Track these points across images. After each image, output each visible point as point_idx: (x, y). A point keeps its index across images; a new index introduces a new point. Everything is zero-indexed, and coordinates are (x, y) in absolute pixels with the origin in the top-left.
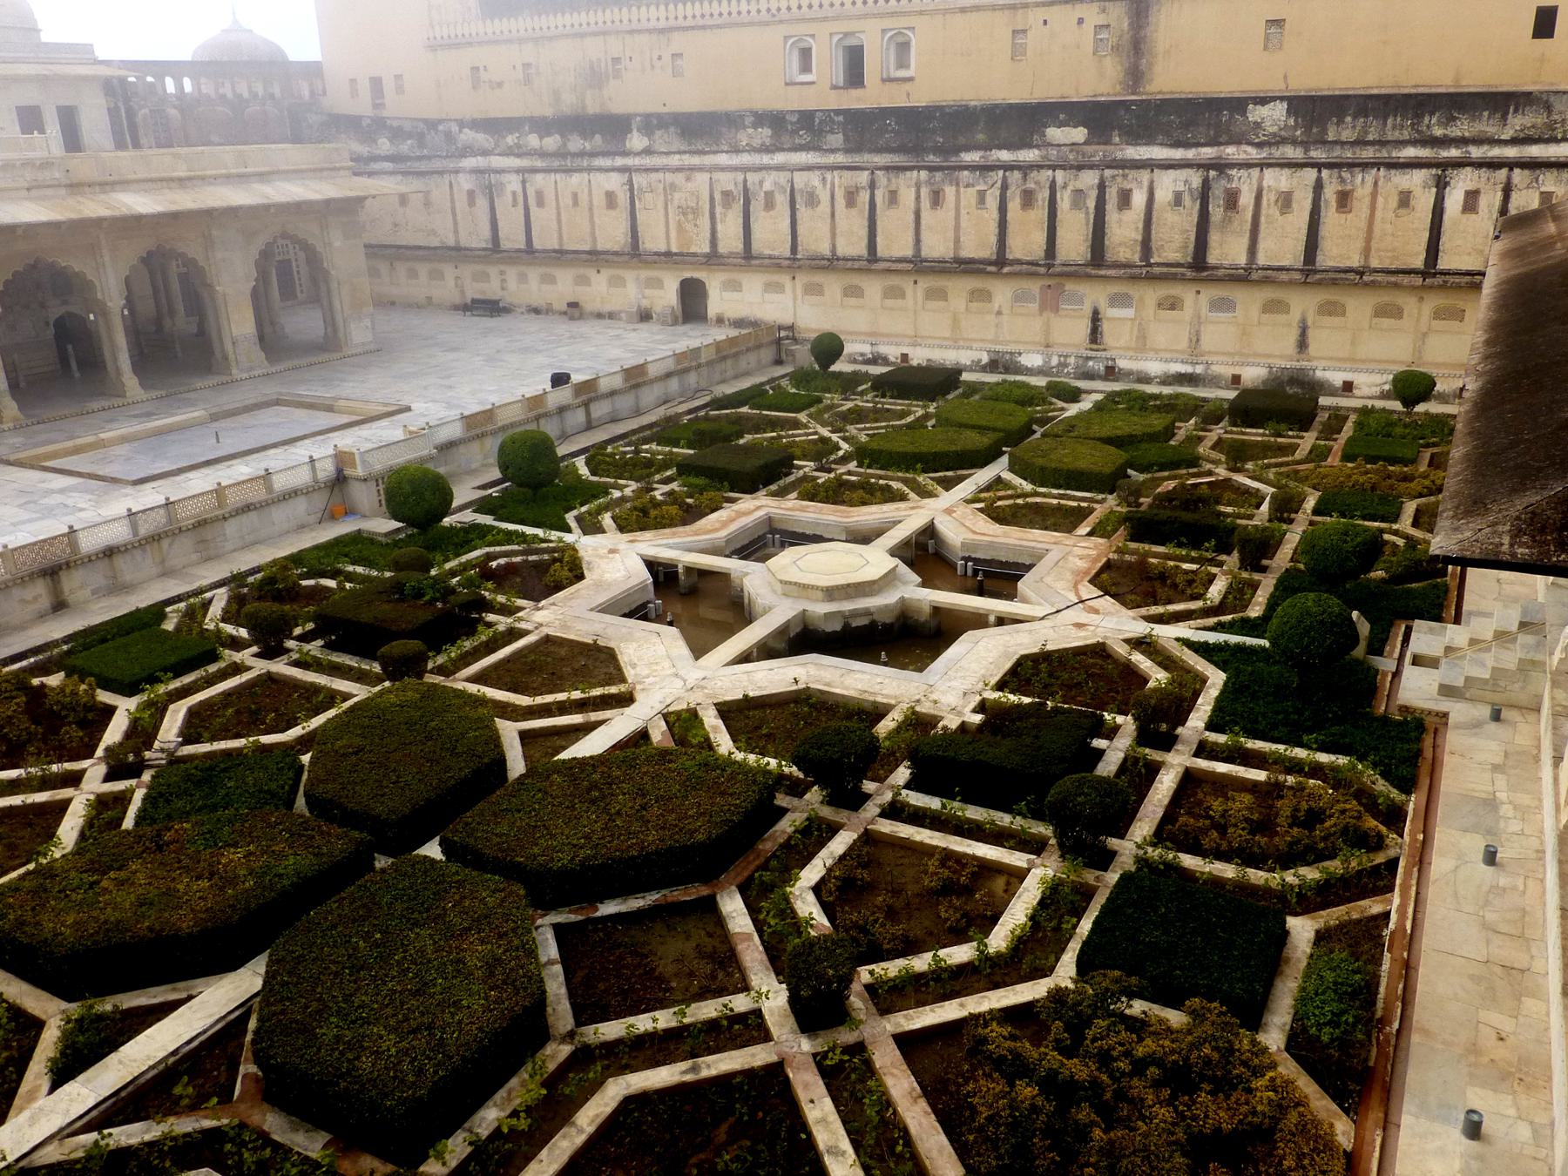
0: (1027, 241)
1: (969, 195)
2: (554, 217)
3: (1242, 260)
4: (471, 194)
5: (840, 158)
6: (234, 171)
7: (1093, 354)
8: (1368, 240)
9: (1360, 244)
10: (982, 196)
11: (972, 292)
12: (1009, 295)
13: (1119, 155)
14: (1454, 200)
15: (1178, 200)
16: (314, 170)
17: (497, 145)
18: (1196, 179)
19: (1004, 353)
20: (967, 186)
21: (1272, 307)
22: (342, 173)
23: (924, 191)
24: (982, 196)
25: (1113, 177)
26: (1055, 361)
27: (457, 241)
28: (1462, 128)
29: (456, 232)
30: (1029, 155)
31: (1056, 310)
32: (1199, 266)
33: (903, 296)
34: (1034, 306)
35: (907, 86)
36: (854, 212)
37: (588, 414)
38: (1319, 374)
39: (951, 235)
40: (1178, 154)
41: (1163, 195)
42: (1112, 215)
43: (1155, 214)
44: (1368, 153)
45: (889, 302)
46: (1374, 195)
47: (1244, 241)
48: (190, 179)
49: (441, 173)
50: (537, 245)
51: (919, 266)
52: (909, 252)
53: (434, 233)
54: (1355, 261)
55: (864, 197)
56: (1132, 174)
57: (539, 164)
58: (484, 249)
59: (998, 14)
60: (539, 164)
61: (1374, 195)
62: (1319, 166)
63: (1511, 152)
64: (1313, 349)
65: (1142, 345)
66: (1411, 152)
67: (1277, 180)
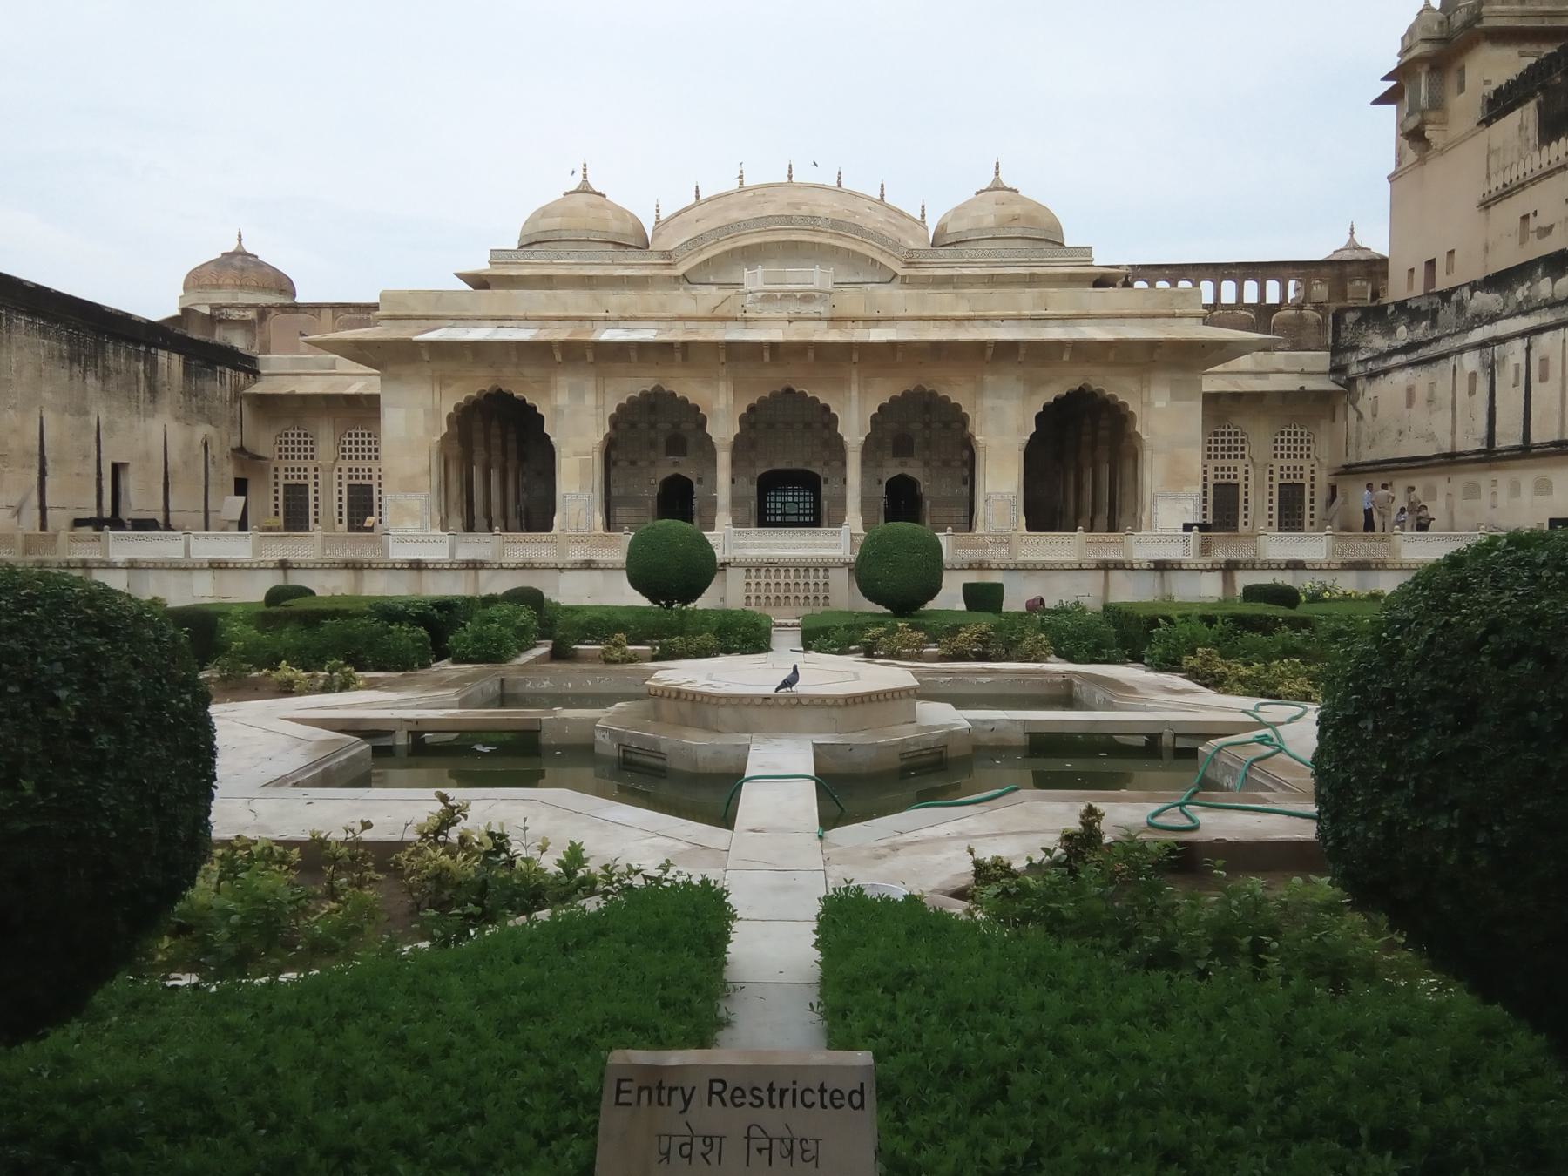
2: (1558, 394)
4: (1473, 375)
6: (1027, 312)
16: (1142, 316)
17: (1505, 305)
22: (1186, 320)
27: (1453, 446)
29: (1453, 432)
37: (1228, 583)
48: (969, 319)
49: (1445, 356)
50: (1536, 438)
53: (1431, 437)
57: (1547, 318)
58: (1478, 452)
60: (1547, 318)
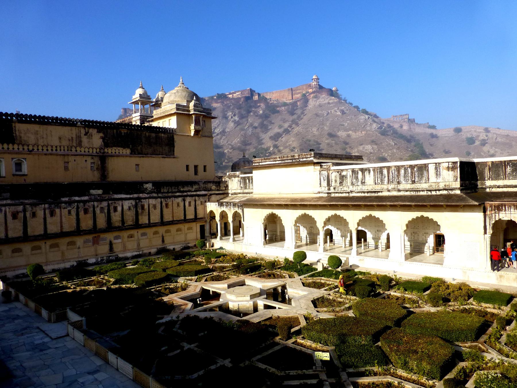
0: (87, 223)
1: (65, 212)
3: (147, 222)
5: (9, 202)
7: (112, 255)
8: (173, 214)
9: (171, 215)
10: (69, 212)
11: (68, 243)
12: (82, 241)
13: (113, 197)
14: (187, 204)
15: (130, 208)
18: (133, 202)
19: (82, 261)
20: (64, 208)
21: (156, 233)
23: (47, 212)
24: (69, 212)
25: (112, 203)
26: (99, 260)
28: (186, 189)
30: (86, 198)
31: (98, 243)
32: (137, 226)
33: (40, 248)
34: (91, 244)
35: (25, 177)
36: (16, 221)
38: (168, 247)
39: (59, 225)
40: (128, 196)
41: (126, 207)
42: (112, 214)
43: (124, 213)
44: (170, 194)
45: (34, 252)
46: (172, 204)
47: (147, 217)
51: (46, 236)
52: (42, 233)
54: (171, 219)
55: (21, 215)
56: (117, 202)
59: (59, 157)
61: (172, 204)
62: (161, 198)
63: (195, 193)
64: (166, 242)
65: (125, 250)
66: (178, 194)
67: (152, 202)
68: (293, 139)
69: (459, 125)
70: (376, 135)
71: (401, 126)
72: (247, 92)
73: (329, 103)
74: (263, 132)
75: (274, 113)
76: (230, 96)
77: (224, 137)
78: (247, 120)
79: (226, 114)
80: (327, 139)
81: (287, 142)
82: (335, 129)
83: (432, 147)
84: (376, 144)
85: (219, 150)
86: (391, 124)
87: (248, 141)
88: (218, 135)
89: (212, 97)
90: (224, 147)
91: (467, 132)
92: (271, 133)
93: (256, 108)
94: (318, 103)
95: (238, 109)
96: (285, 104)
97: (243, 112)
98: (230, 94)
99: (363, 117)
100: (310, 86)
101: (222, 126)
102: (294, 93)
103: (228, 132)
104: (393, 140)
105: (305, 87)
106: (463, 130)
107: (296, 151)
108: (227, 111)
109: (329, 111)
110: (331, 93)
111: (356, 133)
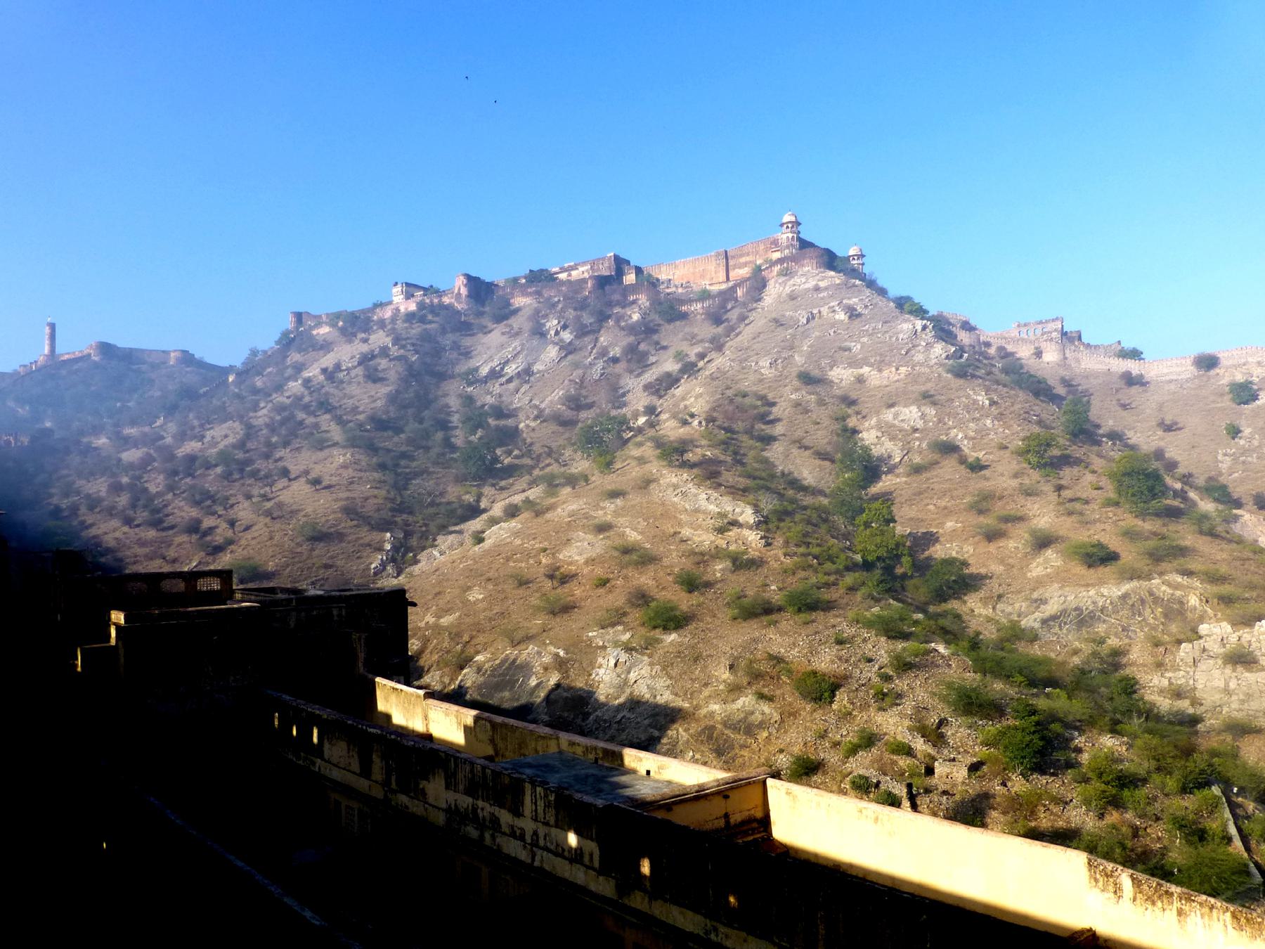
68: (699, 390)
69: (1209, 349)
70: (940, 375)
71: (1039, 354)
72: (606, 265)
73: (817, 289)
74: (631, 372)
75: (670, 321)
76: (563, 276)
77: (525, 387)
78: (597, 340)
79: (544, 325)
80: (797, 390)
81: (683, 399)
82: (824, 362)
83: (1125, 413)
84: (934, 404)
85: (502, 423)
86: (1010, 348)
87: (586, 397)
88: (510, 380)
89: (515, 280)
90: (521, 416)
91: (1236, 367)
92: (650, 376)
93: (623, 307)
94: (788, 290)
95: (575, 309)
96: (705, 295)
97: (588, 319)
98: (563, 270)
99: (907, 326)
100: (775, 243)
101: (527, 355)
102: (731, 263)
103: (539, 372)
104: (987, 391)
105: (762, 247)
106: (1224, 362)
107: (696, 423)
108: (546, 316)
109: (815, 311)
110: (830, 260)
111: (880, 371)
